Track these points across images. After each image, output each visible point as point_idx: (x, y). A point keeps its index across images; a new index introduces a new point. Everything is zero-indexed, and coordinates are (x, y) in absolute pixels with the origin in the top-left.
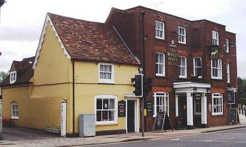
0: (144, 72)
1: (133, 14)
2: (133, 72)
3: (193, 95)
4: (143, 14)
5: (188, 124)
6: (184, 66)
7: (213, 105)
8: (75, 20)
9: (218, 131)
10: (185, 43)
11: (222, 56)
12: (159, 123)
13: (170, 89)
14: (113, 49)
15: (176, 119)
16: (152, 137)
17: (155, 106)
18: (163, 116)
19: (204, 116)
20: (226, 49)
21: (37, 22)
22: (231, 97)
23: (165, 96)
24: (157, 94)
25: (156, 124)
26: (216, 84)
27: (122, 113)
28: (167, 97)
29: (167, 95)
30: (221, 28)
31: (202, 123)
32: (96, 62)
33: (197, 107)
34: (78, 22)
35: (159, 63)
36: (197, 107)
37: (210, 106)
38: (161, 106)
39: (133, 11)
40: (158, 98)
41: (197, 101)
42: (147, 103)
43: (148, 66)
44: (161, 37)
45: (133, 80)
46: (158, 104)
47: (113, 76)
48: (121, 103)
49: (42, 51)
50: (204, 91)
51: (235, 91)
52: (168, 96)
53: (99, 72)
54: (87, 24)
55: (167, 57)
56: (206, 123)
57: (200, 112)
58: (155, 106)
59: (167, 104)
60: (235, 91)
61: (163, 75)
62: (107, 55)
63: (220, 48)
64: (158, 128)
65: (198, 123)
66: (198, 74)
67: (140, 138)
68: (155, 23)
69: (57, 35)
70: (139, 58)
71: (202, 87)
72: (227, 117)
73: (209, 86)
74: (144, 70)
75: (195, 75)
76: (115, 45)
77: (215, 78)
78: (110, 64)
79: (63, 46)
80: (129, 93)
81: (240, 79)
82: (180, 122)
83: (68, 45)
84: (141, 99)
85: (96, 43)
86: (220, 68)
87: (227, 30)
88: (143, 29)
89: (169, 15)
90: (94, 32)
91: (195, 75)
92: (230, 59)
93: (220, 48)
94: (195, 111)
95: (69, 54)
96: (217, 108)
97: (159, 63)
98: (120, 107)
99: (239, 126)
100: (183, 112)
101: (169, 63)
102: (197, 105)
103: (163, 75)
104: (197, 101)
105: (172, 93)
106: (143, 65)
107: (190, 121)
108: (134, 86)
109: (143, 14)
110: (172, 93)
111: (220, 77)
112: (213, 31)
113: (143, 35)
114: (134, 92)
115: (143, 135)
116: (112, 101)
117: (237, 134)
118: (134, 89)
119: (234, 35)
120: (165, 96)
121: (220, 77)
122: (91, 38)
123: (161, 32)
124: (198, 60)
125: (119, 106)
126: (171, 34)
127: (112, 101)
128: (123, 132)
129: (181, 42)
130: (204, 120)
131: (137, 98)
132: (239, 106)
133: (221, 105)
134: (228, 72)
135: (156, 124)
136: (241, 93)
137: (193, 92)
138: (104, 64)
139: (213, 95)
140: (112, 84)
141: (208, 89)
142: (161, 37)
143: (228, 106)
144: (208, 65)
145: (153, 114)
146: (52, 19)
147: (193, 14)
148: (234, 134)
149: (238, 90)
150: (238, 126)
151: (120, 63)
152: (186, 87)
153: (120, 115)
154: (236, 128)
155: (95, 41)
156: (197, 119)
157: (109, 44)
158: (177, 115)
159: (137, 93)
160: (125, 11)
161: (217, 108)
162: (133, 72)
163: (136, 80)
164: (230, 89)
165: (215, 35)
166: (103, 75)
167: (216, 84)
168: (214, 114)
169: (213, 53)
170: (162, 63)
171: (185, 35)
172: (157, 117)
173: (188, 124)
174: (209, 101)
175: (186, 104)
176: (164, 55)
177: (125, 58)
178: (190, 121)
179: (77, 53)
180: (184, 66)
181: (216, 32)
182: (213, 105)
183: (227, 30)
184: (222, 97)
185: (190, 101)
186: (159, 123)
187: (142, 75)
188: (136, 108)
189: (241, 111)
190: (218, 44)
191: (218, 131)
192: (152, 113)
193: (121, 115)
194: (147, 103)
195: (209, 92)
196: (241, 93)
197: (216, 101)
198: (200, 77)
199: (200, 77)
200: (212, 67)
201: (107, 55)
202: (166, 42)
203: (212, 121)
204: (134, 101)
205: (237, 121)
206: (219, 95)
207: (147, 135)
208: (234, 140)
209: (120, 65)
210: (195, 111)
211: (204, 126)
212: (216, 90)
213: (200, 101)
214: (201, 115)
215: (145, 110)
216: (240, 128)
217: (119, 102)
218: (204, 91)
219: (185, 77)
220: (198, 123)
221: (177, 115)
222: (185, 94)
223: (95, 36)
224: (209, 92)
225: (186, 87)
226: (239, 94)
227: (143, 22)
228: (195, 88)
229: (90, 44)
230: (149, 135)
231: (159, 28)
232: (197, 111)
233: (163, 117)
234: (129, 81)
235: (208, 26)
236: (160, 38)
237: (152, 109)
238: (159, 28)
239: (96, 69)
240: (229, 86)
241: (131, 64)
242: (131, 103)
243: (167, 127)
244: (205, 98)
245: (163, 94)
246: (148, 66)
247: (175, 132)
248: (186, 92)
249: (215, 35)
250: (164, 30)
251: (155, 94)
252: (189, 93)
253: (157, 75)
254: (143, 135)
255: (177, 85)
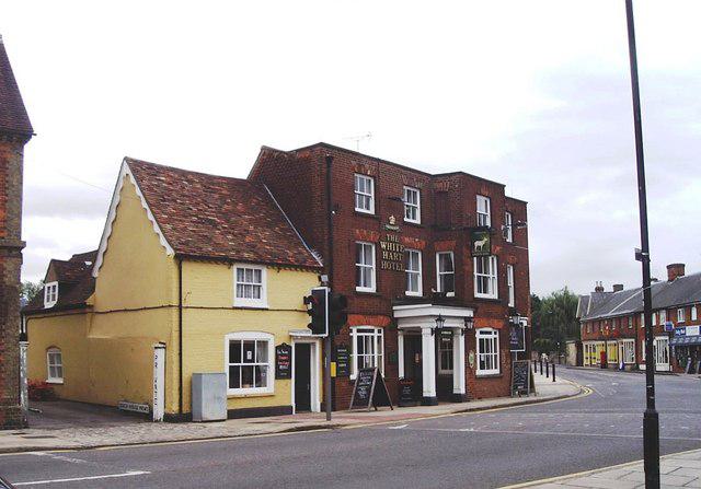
0: (330, 284)
1: (307, 160)
2: (308, 283)
3: (436, 332)
4: (330, 160)
5: (424, 395)
6: (416, 271)
7: (478, 353)
8: (184, 173)
9: (488, 408)
10: (418, 221)
11: (498, 248)
12: (362, 393)
13: (386, 321)
14: (265, 235)
15: (400, 384)
16: (348, 421)
17: (355, 355)
18: (372, 377)
19: (459, 377)
20: (506, 235)
21: (102, 177)
22: (517, 336)
23: (376, 334)
24: (359, 331)
25: (357, 395)
26: (484, 310)
27: (284, 371)
28: (379, 338)
29: (379, 332)
30: (495, 190)
31: (455, 392)
32: (228, 262)
33: (445, 358)
34: (190, 177)
35: (362, 265)
36: (445, 358)
37: (472, 355)
38: (367, 356)
39: (308, 153)
40: (360, 338)
41: (444, 345)
42: (337, 349)
43: (340, 271)
44: (368, 209)
45: (307, 301)
46: (360, 351)
47: (264, 292)
48: (282, 349)
49: (108, 254)
50: (460, 324)
51: (525, 324)
52: (382, 334)
53: (236, 283)
54: (210, 182)
55: (379, 251)
56: (463, 391)
57: (452, 368)
58: (355, 355)
59: (380, 352)
60: (525, 324)
61: (372, 289)
62: (252, 247)
63: (494, 233)
64: (360, 404)
65: (445, 392)
66: (447, 288)
67: (323, 424)
68: (354, 178)
69: (145, 205)
70: (321, 254)
71: (455, 316)
72: (508, 379)
73: (469, 313)
74: (330, 278)
75: (439, 291)
76: (269, 226)
77: (482, 295)
78: (257, 267)
79: (156, 228)
80: (300, 327)
81: (536, 299)
82: (407, 391)
83: (169, 226)
84: (323, 341)
85: (227, 221)
86: (493, 275)
87: (508, 193)
88: (329, 192)
89: (384, 162)
90: (223, 198)
91: (439, 291)
92: (516, 257)
93: (494, 233)
94: (440, 367)
95: (172, 246)
96: (488, 360)
97: (362, 265)
98: (281, 358)
99: (535, 399)
100: (415, 368)
101: (385, 265)
102: (444, 355)
103: (372, 289)
104: (444, 345)
105: (391, 329)
106: (327, 269)
107: (429, 389)
108: (309, 312)
109: (330, 160)
110: (391, 329)
111: (493, 294)
112: (478, 197)
113: (329, 205)
114: (309, 326)
115: (329, 418)
116: (263, 344)
117: (531, 415)
118: (309, 320)
119: (524, 204)
120: (376, 334)
121: (493, 294)
122: (219, 211)
123: (368, 198)
124: (445, 258)
125: (277, 355)
126: (389, 203)
127: (263, 344)
128: (285, 411)
129: (411, 221)
130: (460, 387)
131: (317, 338)
132: (535, 355)
133: (495, 353)
134: (511, 283)
135: (357, 395)
136: (538, 328)
137: (435, 325)
138: (245, 267)
139: (478, 332)
140: (263, 309)
141: (467, 319)
142: (368, 209)
143: (511, 355)
144: (467, 268)
145: (349, 372)
146: (134, 171)
147: (434, 157)
148: (524, 415)
149: (532, 322)
150: (532, 398)
151: (279, 264)
152: (420, 316)
153: (279, 375)
154: (527, 403)
155: (226, 216)
156: (444, 384)
157: (256, 223)
158: (401, 374)
159: (316, 327)
160: (290, 154)
161: (488, 360)
162: (308, 283)
163: (315, 300)
164: (515, 319)
165: (482, 206)
166: (243, 290)
167: (484, 310)
168: (479, 372)
169: (477, 243)
170: (369, 265)
171: (418, 205)
172: (359, 379)
173: (424, 395)
174: (470, 346)
175: (420, 352)
176: (374, 248)
177: (291, 254)
178: (429, 389)
179: (186, 243)
180: (416, 271)
181: (484, 199)
182: (478, 353)
183: (508, 193)
184: (497, 336)
185: (429, 345)
186: (362, 393)
187: (327, 290)
188: (315, 352)
189: (538, 367)
190: (489, 224)
191: (488, 408)
192: (348, 371)
193: (281, 374)
194: (337, 349)
195: (470, 325)
196: (538, 328)
197: (484, 345)
198: (450, 294)
199: (450, 294)
200: (476, 274)
201: (252, 247)
202: (377, 221)
203: (477, 388)
204: (308, 345)
205: (530, 387)
206: (490, 333)
207: (339, 418)
208: (523, 428)
209: (279, 269)
210: (440, 367)
211: (458, 399)
212: (483, 321)
213: (451, 345)
214: (452, 375)
215: (333, 365)
216: (535, 402)
217: (277, 348)
218: (460, 324)
219: (419, 293)
220: (445, 392)
221: (401, 374)
222: (419, 330)
223: (226, 206)
224: (470, 325)
225: (420, 316)
226: (533, 330)
227: (328, 177)
228: (440, 318)
229: (215, 225)
230: (341, 417)
231: (362, 190)
232: (444, 367)
233: (371, 380)
234: (299, 304)
235: (467, 185)
236: (364, 211)
237: (349, 361)
238: (362, 190)
239: (228, 277)
240: (513, 312)
241: (302, 266)
242: (304, 350)
243: (381, 400)
244: (462, 339)
245: (372, 331)
246: (340, 271)
247: (398, 411)
248: (421, 325)
249: (482, 206)
250: (372, 195)
251: (354, 330)
252: (427, 330)
253: (358, 289)
254: (329, 418)
255: (401, 311)
